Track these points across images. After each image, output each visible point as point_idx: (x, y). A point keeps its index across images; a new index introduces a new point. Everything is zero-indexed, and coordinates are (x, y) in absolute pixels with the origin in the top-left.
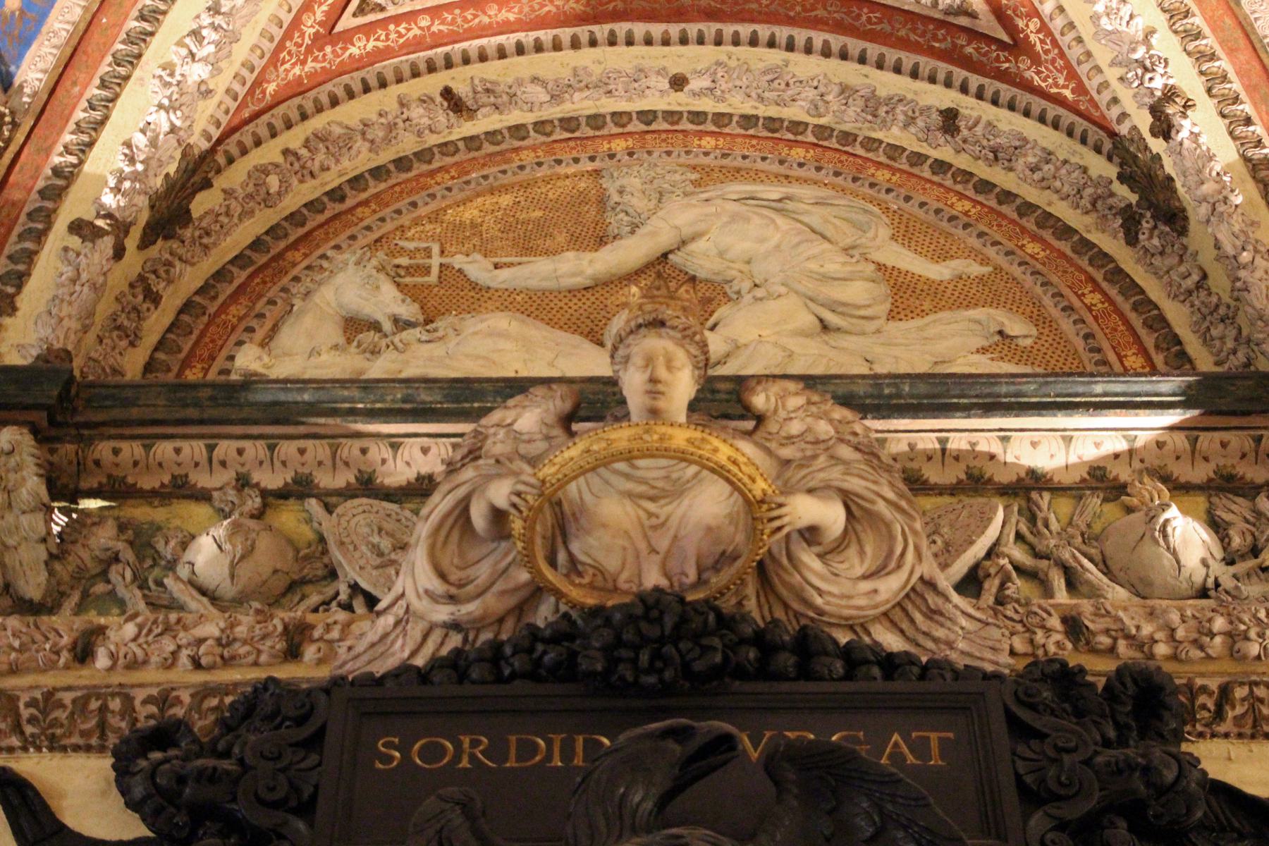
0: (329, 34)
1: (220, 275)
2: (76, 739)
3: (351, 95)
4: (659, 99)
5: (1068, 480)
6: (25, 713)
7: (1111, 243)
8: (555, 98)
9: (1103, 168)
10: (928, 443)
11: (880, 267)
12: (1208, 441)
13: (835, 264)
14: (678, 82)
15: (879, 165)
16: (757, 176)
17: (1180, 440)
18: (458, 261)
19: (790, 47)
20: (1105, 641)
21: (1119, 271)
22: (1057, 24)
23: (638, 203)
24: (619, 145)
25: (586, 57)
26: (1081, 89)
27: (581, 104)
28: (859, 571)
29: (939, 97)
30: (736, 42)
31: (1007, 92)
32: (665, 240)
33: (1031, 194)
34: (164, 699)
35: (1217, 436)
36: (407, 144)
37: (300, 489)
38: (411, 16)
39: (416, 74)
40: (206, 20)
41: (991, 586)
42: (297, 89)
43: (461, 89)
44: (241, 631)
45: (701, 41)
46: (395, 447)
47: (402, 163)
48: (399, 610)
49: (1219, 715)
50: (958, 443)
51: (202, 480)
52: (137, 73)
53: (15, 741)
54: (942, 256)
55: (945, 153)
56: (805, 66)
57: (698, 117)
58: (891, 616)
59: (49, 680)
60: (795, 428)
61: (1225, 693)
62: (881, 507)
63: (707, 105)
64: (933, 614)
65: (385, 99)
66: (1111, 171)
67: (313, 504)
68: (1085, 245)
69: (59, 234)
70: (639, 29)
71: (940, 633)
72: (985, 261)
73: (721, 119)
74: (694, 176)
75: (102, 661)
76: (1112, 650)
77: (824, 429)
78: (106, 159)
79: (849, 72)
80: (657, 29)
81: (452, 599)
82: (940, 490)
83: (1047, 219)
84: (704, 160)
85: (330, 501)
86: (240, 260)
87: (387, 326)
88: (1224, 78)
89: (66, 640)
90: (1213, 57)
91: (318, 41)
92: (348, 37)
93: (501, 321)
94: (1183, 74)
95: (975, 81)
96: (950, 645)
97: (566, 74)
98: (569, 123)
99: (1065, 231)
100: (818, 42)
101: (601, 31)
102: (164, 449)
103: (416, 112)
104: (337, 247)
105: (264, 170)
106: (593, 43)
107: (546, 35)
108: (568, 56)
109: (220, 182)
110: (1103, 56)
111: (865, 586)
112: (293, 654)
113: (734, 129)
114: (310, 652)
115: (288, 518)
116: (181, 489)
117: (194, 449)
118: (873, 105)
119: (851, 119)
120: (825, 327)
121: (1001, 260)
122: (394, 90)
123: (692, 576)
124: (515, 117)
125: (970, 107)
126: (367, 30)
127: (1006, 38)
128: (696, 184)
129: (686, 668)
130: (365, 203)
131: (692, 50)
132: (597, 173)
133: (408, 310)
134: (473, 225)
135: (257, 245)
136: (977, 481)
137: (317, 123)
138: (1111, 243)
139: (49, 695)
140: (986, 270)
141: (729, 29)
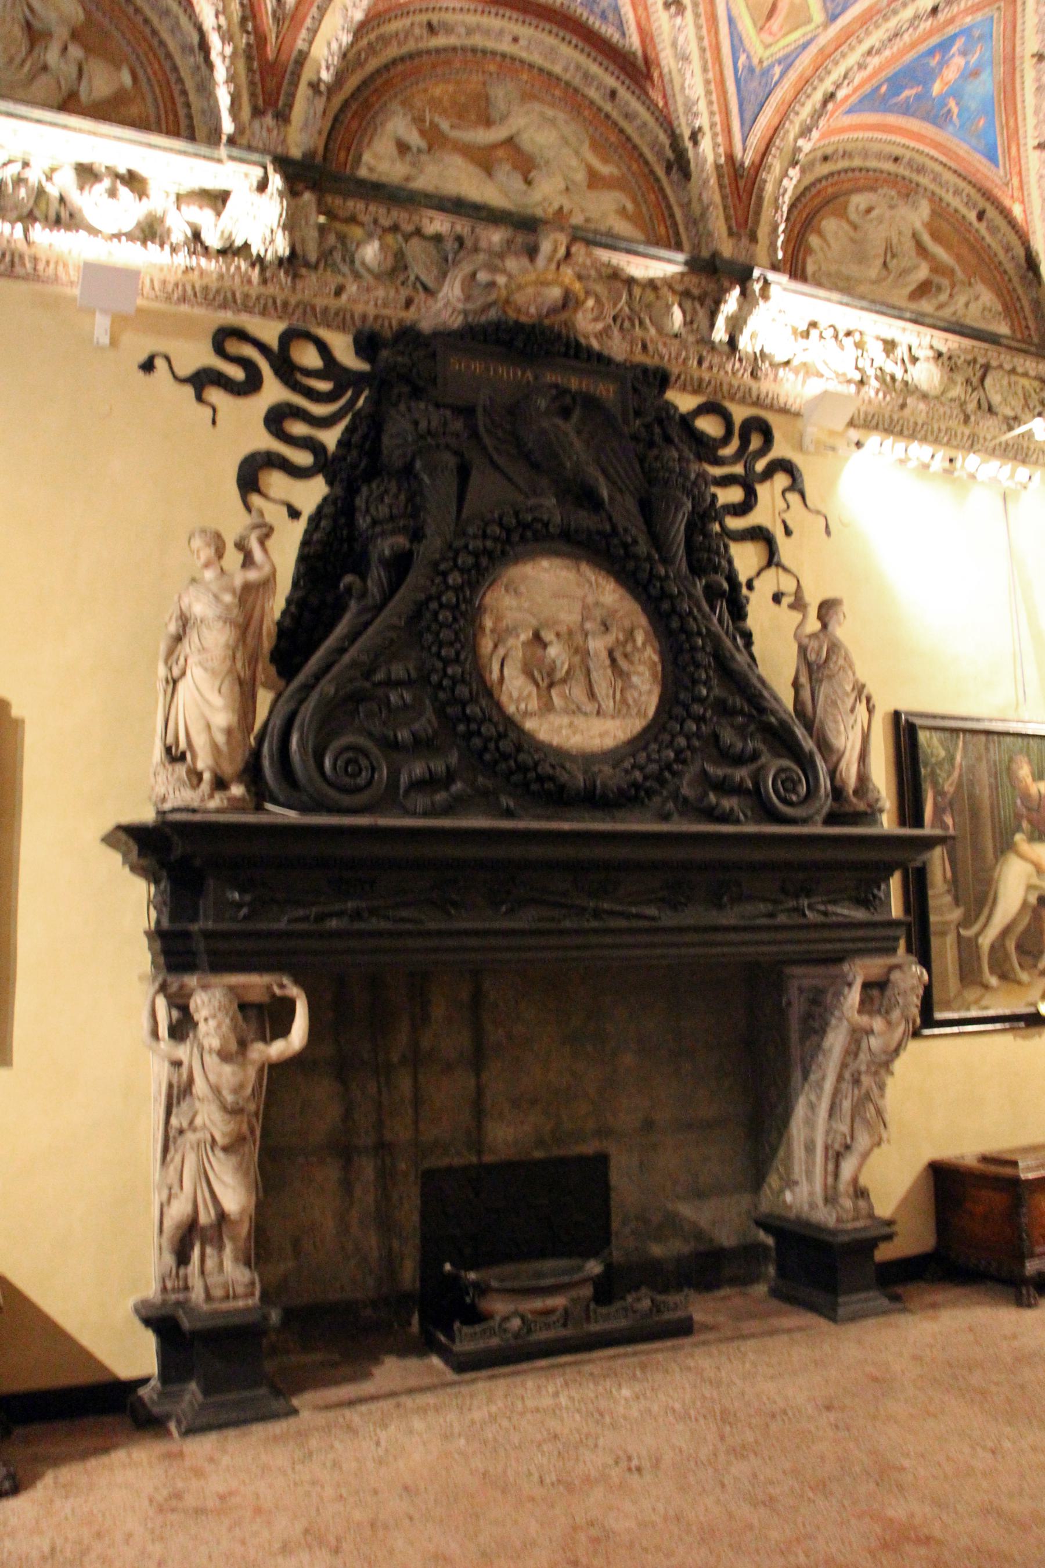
4: (505, 46)
7: (660, 172)
12: (686, 279)
13: (574, 162)
16: (542, 101)
18: (437, 119)
26: (666, 104)
27: (478, 41)
29: (611, 82)
32: (514, 130)
36: (411, 46)
37: (395, 228)
43: (435, 22)
47: (411, 56)
51: (362, 218)
54: (605, 161)
55: (608, 107)
56: (565, 50)
58: (599, 336)
61: (679, 376)
63: (524, 55)
65: (406, 22)
67: (400, 237)
68: (652, 172)
75: (344, 297)
79: (582, 59)
85: (407, 238)
87: (415, 150)
89: (333, 288)
93: (458, 160)
98: (474, 50)
99: (647, 163)
100: (574, 42)
102: (350, 204)
110: (680, 100)
116: (353, 220)
117: (360, 206)
118: (586, 76)
119: (577, 81)
124: (452, 41)
125: (623, 93)
133: (423, 144)
135: (358, 89)
136: (615, 276)
138: (660, 172)
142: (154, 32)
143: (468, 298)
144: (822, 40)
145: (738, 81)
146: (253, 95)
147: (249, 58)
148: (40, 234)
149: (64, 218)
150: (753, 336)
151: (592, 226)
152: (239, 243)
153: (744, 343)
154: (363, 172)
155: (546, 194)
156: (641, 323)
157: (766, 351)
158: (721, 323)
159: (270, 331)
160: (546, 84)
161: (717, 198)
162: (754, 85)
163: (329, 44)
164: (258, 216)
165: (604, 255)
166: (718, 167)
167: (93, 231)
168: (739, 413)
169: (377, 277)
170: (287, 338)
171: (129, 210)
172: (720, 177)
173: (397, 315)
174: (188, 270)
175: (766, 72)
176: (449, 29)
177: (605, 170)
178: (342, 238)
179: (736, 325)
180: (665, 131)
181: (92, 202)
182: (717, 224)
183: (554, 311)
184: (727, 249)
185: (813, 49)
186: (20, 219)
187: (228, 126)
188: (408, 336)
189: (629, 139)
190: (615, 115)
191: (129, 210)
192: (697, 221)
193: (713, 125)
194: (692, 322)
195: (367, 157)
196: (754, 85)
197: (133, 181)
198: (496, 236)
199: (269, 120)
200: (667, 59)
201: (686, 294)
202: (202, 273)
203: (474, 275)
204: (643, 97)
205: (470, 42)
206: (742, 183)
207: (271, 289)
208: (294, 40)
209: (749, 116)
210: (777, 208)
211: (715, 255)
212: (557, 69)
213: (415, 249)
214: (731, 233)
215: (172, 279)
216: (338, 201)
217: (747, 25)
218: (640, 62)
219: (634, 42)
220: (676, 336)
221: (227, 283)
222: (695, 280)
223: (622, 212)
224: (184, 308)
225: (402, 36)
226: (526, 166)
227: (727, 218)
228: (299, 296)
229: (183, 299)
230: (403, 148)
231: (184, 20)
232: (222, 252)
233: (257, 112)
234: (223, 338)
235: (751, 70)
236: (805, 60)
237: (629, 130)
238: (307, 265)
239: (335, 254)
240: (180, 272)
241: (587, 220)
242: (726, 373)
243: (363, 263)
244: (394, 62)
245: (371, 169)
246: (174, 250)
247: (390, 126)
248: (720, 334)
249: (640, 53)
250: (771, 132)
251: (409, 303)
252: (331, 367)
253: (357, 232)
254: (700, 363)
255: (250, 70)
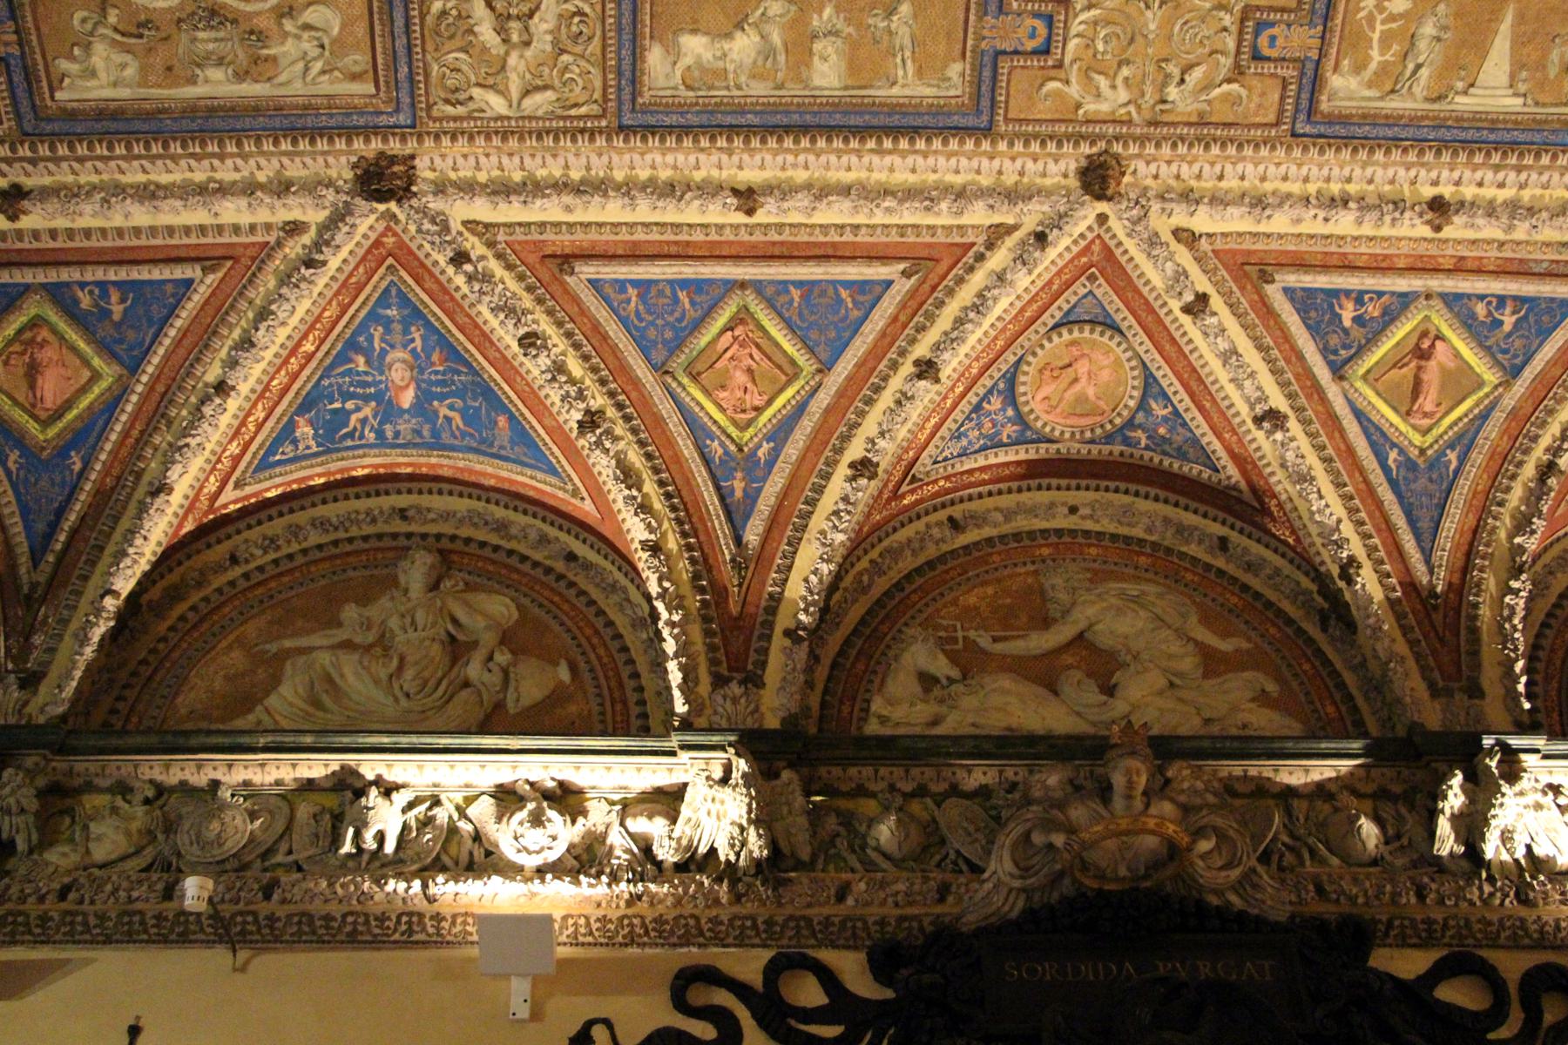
0: (896, 495)
1: (847, 642)
2: (842, 942)
3: (903, 525)
4: (1062, 521)
5: (1306, 791)
6: (817, 928)
7: (1313, 630)
8: (1007, 519)
9: (1306, 583)
10: (1238, 772)
11: (1197, 643)
12: (1374, 772)
13: (1175, 647)
14: (1073, 510)
15: (1186, 569)
16: (1121, 578)
17: (1362, 772)
18: (972, 634)
19: (1137, 494)
20: (1334, 896)
21: (1319, 650)
22: (1288, 506)
23: (1063, 596)
24: (1046, 551)
25: (1025, 497)
26: (1298, 540)
27: (1022, 523)
28: (1220, 864)
29: (1218, 529)
30: (1107, 489)
31: (1257, 533)
32: (1082, 625)
33: (1271, 595)
34: (882, 922)
35: (1379, 770)
36: (932, 551)
37: (921, 792)
38: (936, 481)
39: (935, 510)
40: (842, 506)
41: (1275, 858)
42: (878, 527)
44: (916, 887)
45: (1087, 489)
46: (970, 772)
47: (930, 564)
48: (994, 879)
49: (1386, 934)
50: (1253, 772)
51: (873, 787)
52: (806, 536)
53: (812, 942)
54: (1225, 634)
55: (1220, 563)
56: (1144, 505)
57: (1087, 533)
58: (1238, 887)
59: (826, 911)
60: (1186, 785)
61: (1389, 925)
62: (1231, 833)
63: (1089, 525)
64: (1255, 886)
65: (919, 525)
66: (1314, 588)
67: (928, 800)
68: (1300, 631)
69: (778, 641)
70: (1054, 482)
71: (1259, 896)
72: (1249, 640)
73: (1100, 535)
74: (1089, 575)
75: (850, 901)
76: (1337, 900)
77: (1199, 785)
78: (795, 589)
79: (1169, 510)
80: (1063, 482)
81: (1022, 877)
82: (1244, 796)
83: (1280, 612)
84: (1092, 565)
85: (939, 800)
86: (855, 632)
87: (944, 681)
88: (1376, 549)
89: (833, 891)
90: (1370, 537)
91: (889, 500)
92: (903, 496)
93: (1006, 682)
94: (1356, 548)
95: (1239, 524)
96: (1264, 902)
97: (1013, 505)
98: (1017, 536)
99: (1290, 621)
100: (1152, 494)
101: (1034, 483)
102: (853, 771)
103: (935, 532)
104: (906, 624)
105: (860, 574)
106: (1029, 489)
107: (1003, 486)
108: (1014, 497)
109: (842, 585)
110: (1314, 530)
111: (1223, 874)
112: (942, 900)
113: (1106, 543)
114: (950, 899)
115: (915, 807)
116: (861, 791)
117: (868, 771)
118: (1181, 529)
119: (1169, 540)
120: (1172, 685)
121: (1259, 640)
122: (925, 520)
123: (1142, 871)
124: (988, 532)
125: (1234, 536)
126: (912, 491)
127: (1256, 505)
128: (1091, 580)
129: (1141, 917)
130: (915, 591)
131: (1082, 493)
132: (1036, 572)
133: (955, 673)
134: (976, 608)
135: (863, 622)
136: (1262, 790)
137: (886, 543)
138: (1313, 630)
139: (827, 918)
140: (1250, 646)
141: (1104, 484)
142: (600, 612)
143: (1025, 871)
144: (1509, 401)
145: (1393, 484)
146: (714, 662)
147: (706, 619)
148: (444, 888)
149: (480, 860)
150: (1506, 837)
151: (1215, 729)
152: (703, 849)
153: (1491, 848)
154: (873, 728)
155: (1144, 699)
156: (1313, 852)
157: (1539, 851)
158: (1444, 826)
159: (749, 965)
160: (1124, 555)
161: (1402, 647)
162: (1422, 482)
163: (806, 580)
164: (719, 813)
165: (1235, 768)
166: (1392, 603)
167: (511, 870)
168: (1513, 965)
169: (897, 863)
170: (773, 970)
171: (560, 835)
172: (1399, 617)
173: (928, 911)
174: (634, 899)
175: (1436, 462)
176: (978, 520)
177: (1226, 646)
178: (847, 820)
179: (1472, 826)
180: (1307, 574)
181: (509, 836)
182: (1410, 684)
183: (1155, 865)
184: (1432, 716)
185: (1498, 416)
186: (415, 874)
187: (680, 707)
188: (945, 941)
189: (1257, 595)
190: (1231, 569)
191: (560, 835)
192: (1378, 686)
193: (1371, 550)
194: (1398, 837)
195: (877, 705)
196: (1422, 485)
197: (567, 799)
198: (1053, 778)
199: (735, 689)
200: (1281, 484)
201: (1382, 795)
202: (654, 900)
203: (1027, 837)
204: (1266, 538)
205: (1007, 529)
206: (1440, 618)
207: (748, 908)
208: (764, 584)
209: (1425, 524)
210: (1505, 638)
211: (1414, 727)
212: (1138, 532)
213: (953, 811)
214: (1434, 691)
215: (614, 915)
216: (837, 771)
217: (1386, 414)
218: (1247, 496)
219: (1232, 472)
220: (1375, 862)
221: (688, 909)
222: (1389, 773)
223: (1263, 698)
224: (634, 951)
225: (916, 545)
226: (1102, 665)
227: (1424, 670)
228: (789, 910)
229: (631, 940)
230: (927, 681)
231: (632, 589)
232: (681, 868)
233: (719, 681)
234: (684, 983)
235: (1411, 465)
236: (1492, 430)
237: (1255, 583)
238: (799, 865)
239: (838, 840)
240: (622, 904)
241: (1207, 721)
242: (1472, 903)
243: (877, 849)
244: (908, 577)
245: (883, 720)
246: (614, 878)
247: (907, 658)
248: (1447, 842)
249: (1243, 485)
250: (1468, 537)
251: (943, 892)
252: (841, 1002)
253: (870, 806)
254: (1421, 897)
255: (708, 633)
